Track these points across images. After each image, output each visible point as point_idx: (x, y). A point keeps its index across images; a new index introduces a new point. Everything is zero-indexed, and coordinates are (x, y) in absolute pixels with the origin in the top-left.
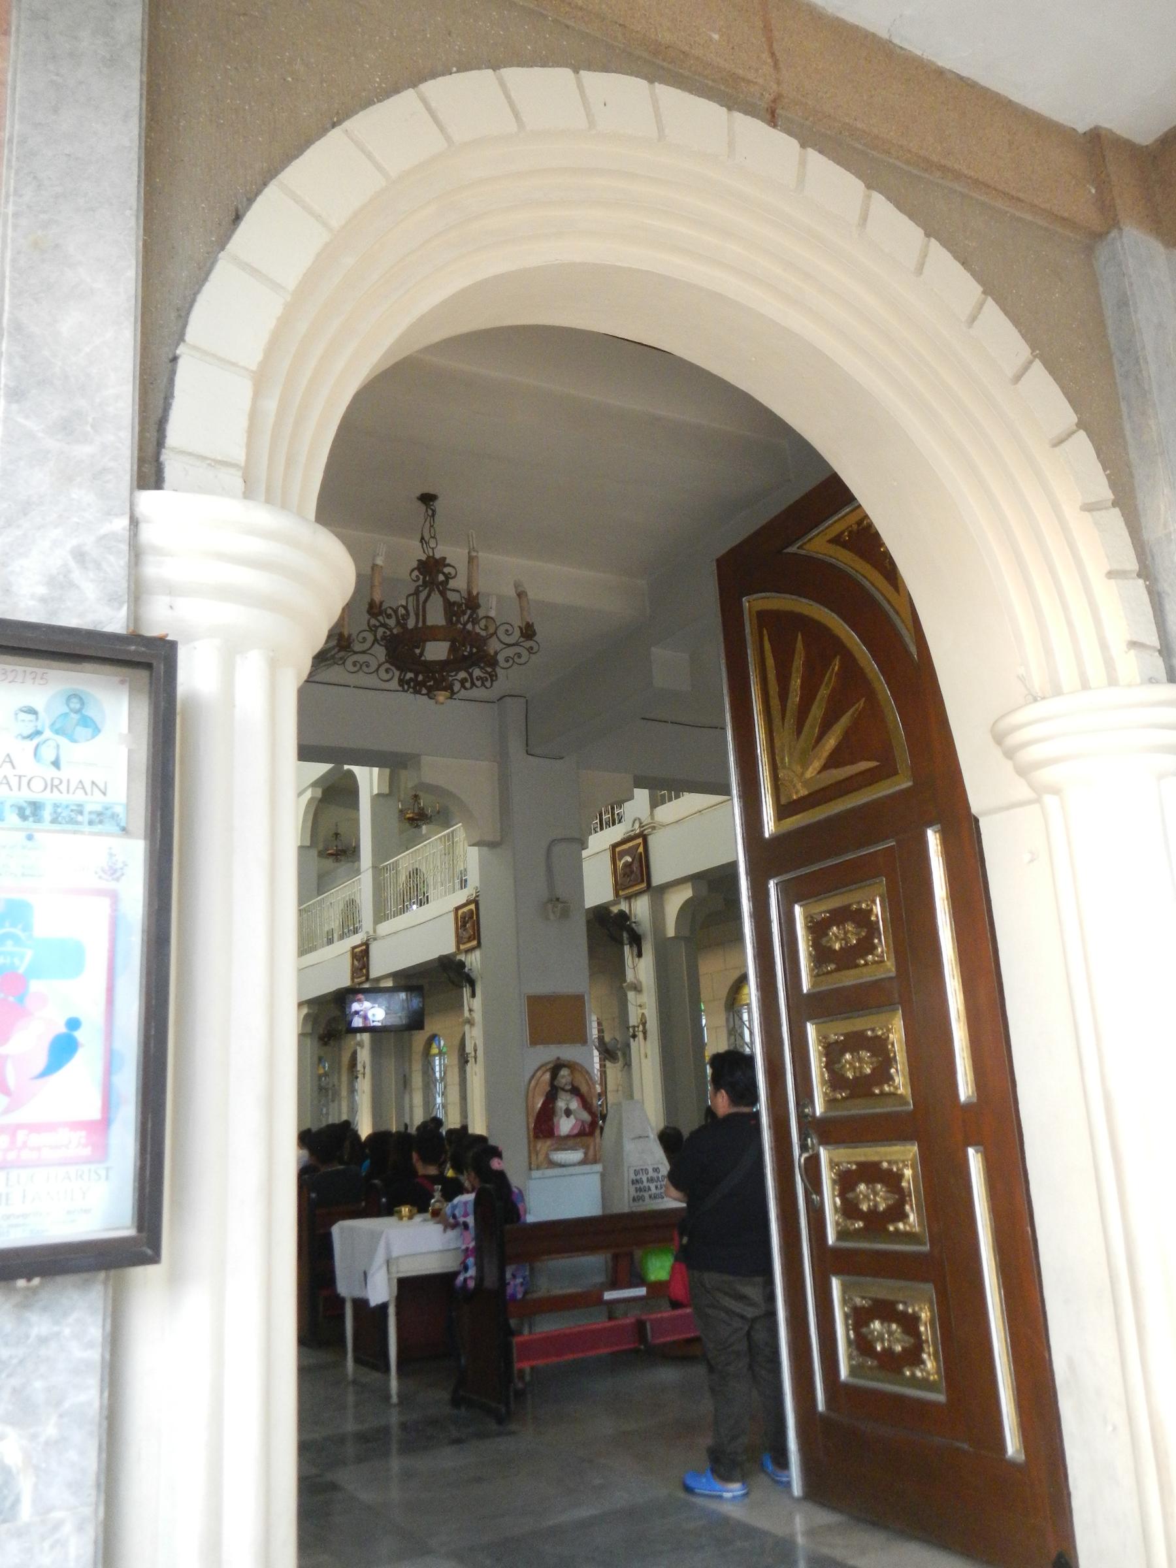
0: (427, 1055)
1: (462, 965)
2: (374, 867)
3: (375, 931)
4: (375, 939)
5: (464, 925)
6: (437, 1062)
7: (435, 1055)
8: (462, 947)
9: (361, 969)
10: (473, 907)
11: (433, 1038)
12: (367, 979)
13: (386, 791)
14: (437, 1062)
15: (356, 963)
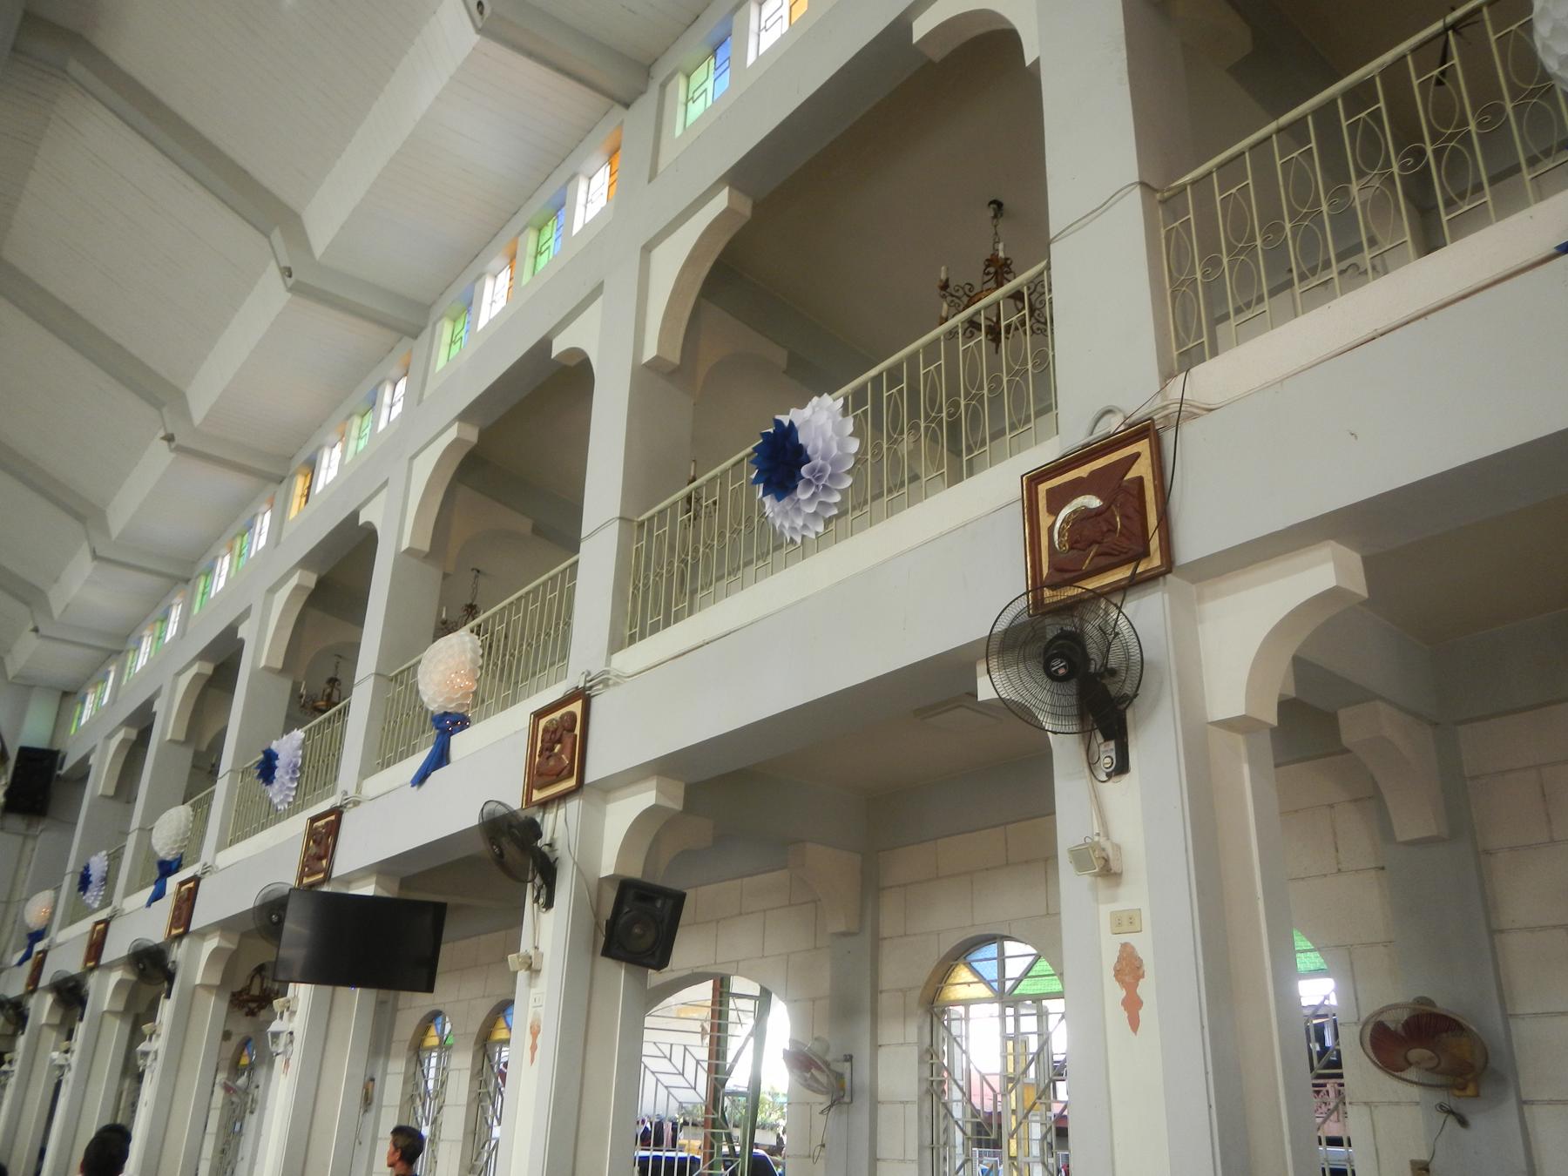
0: (417, 1051)
1: (534, 830)
2: (377, 674)
3: (359, 788)
4: (357, 803)
5: (548, 749)
6: (434, 1062)
7: (431, 1049)
8: (537, 796)
9: (320, 858)
10: (576, 707)
11: (434, 1016)
12: (327, 878)
13: (425, 546)
14: (434, 1062)
15: (313, 849)
